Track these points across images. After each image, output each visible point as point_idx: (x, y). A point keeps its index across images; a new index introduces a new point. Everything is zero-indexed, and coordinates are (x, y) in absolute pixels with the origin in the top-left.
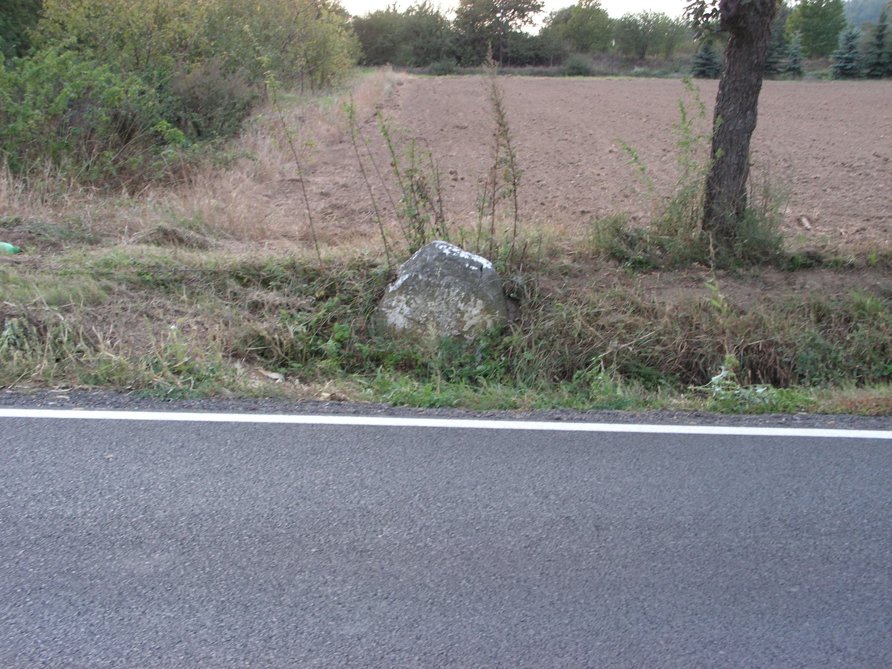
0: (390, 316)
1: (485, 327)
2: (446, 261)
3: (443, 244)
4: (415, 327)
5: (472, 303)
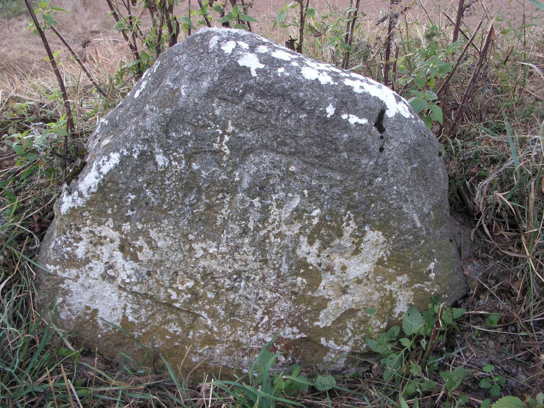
0: (74, 287)
1: (391, 312)
2: (250, 97)
3: (237, 37)
4: (159, 318)
5: (346, 241)
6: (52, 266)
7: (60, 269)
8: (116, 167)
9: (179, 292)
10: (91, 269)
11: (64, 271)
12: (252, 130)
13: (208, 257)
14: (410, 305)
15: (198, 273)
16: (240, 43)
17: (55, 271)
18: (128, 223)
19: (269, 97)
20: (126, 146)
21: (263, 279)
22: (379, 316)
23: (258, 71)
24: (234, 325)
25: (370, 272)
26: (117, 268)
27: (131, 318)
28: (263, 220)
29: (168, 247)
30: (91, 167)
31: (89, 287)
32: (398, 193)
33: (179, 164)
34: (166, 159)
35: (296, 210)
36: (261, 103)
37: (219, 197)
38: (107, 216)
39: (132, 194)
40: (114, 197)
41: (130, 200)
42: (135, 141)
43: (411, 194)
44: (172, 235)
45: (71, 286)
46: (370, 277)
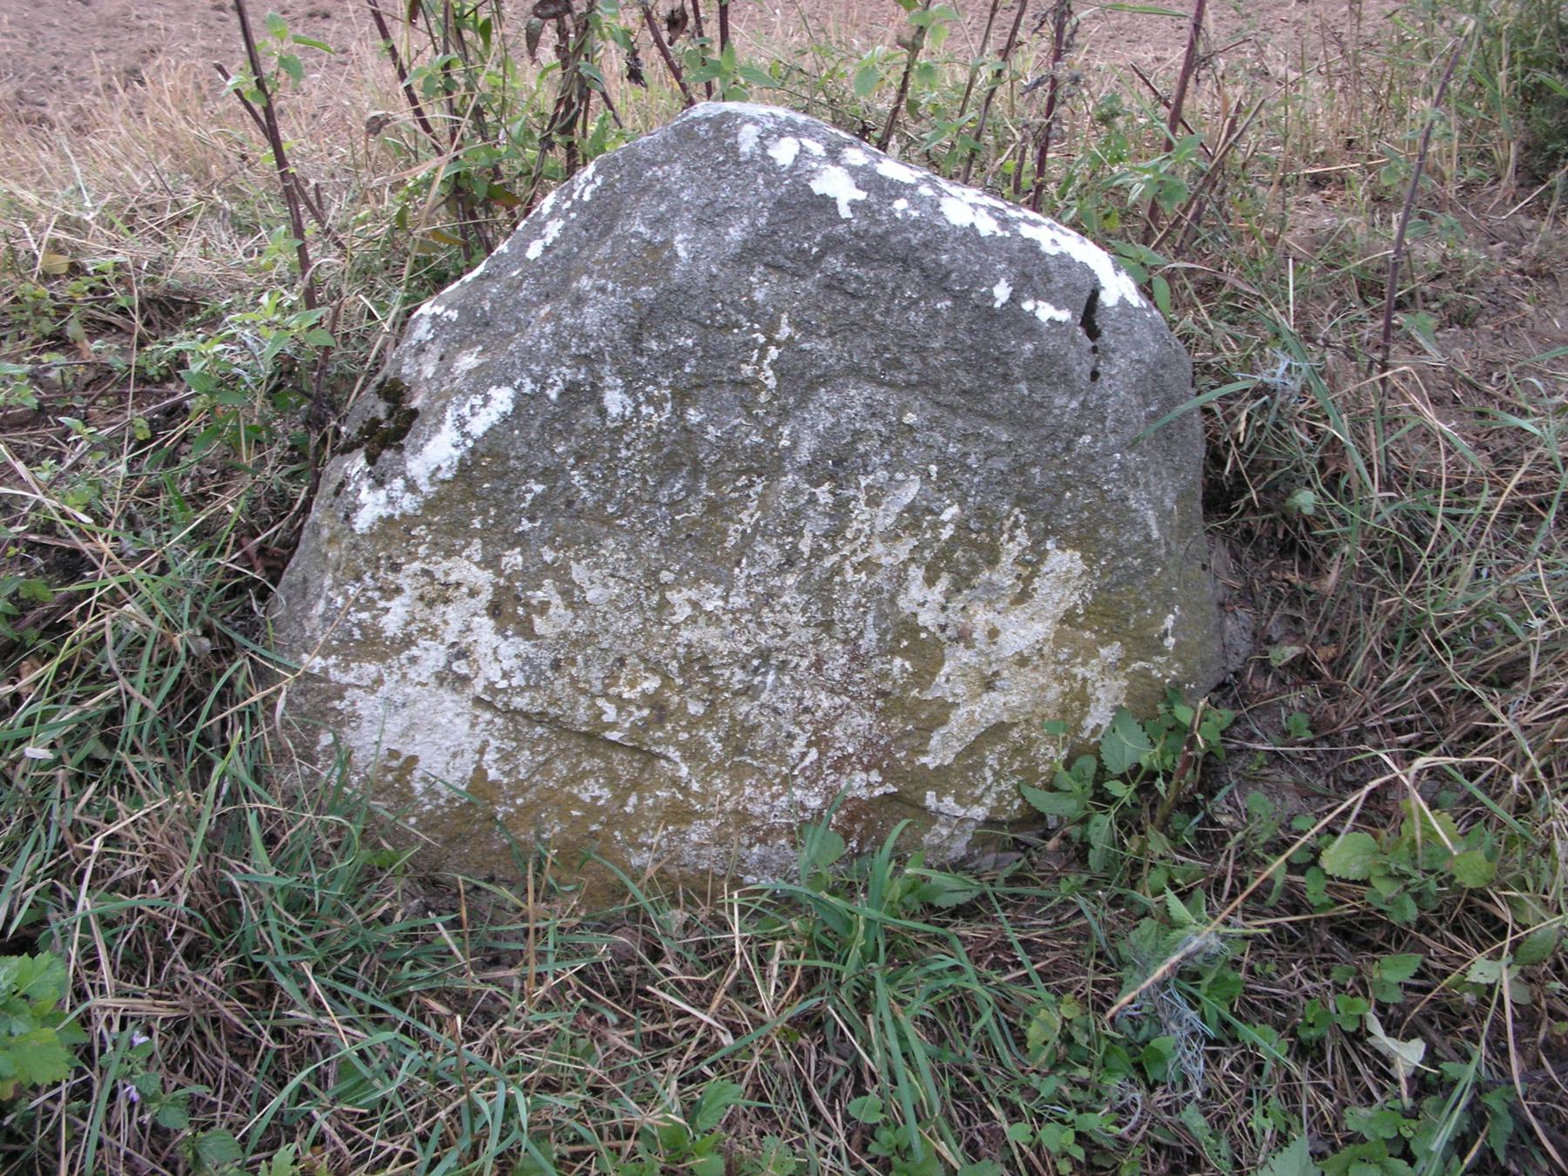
0: (367, 706)
1: (1078, 727)
2: (835, 263)
4: (561, 768)
5: (1004, 576)
6: (318, 659)
7: (336, 666)
8: (506, 421)
9: (621, 703)
10: (413, 660)
11: (347, 669)
12: (832, 334)
13: (702, 621)
14: (1118, 709)
15: (674, 657)
16: (808, 143)
17: (325, 670)
18: (518, 550)
19: (875, 264)
20: (530, 370)
21: (818, 664)
23: (854, 205)
24: (738, 774)
25: (1046, 640)
26: (476, 656)
27: (493, 774)
28: (834, 534)
29: (610, 601)
30: (441, 422)
31: (404, 705)
32: (1123, 467)
33: (656, 411)
34: (629, 401)
35: (910, 508)
36: (857, 277)
37: (739, 484)
38: (473, 534)
39: (538, 482)
40: (493, 490)
41: (529, 497)
42: (555, 359)
43: (1145, 469)
44: (622, 573)
45: (359, 704)
46: (1046, 650)
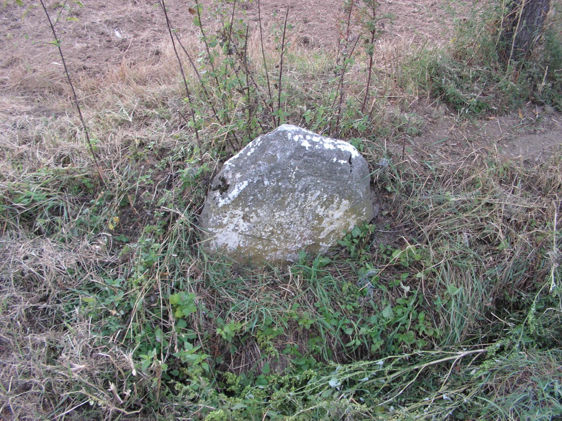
1: (348, 229)
2: (306, 157)
5: (335, 205)
9: (266, 232)
10: (228, 228)
21: (301, 223)
22: (343, 232)
23: (309, 147)
27: (241, 245)
28: (304, 201)
32: (356, 186)
35: (318, 196)
42: (255, 176)
